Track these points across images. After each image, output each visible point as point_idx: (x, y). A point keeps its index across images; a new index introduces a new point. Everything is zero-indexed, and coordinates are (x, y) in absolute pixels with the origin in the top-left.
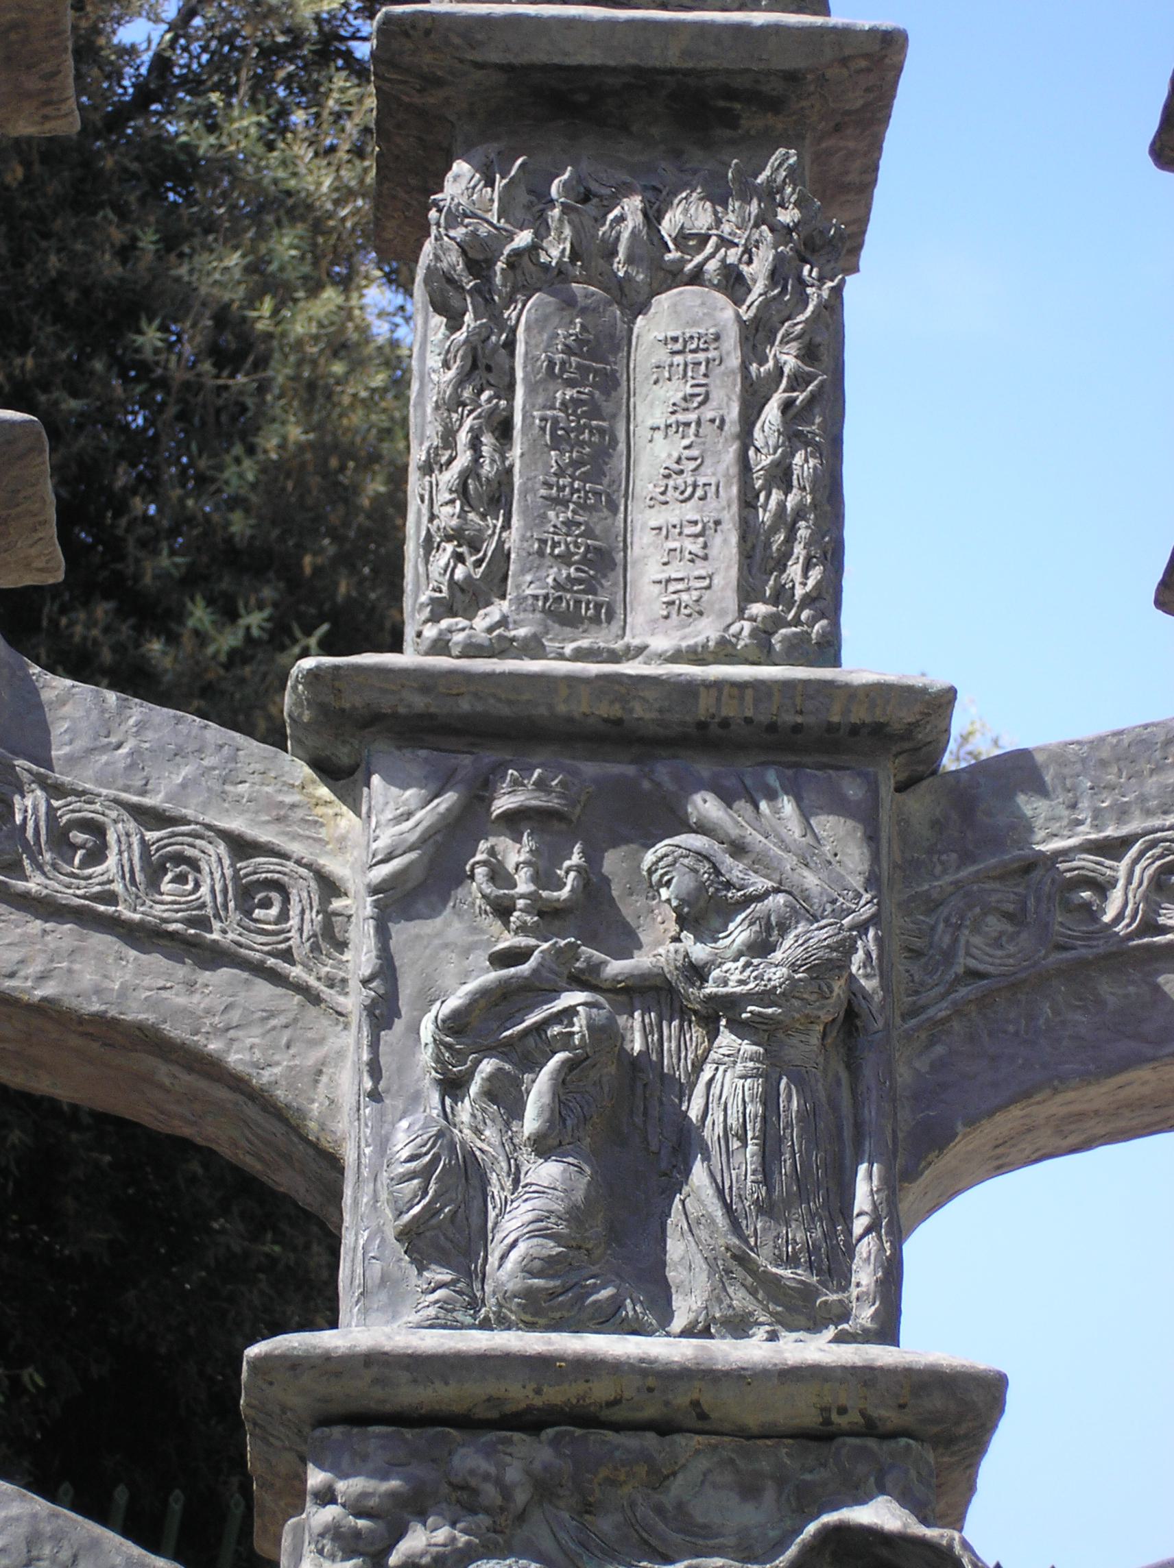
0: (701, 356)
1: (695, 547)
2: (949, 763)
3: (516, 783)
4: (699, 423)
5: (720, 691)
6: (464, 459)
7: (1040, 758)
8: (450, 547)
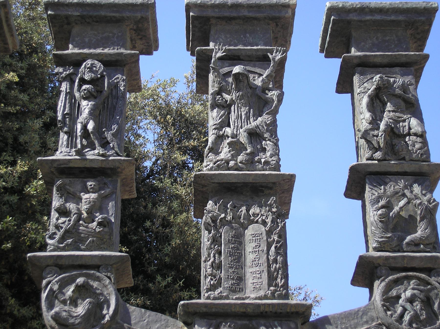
0: (258, 238)
1: (259, 276)
2: (312, 319)
3: (224, 326)
4: (258, 251)
5: (265, 306)
6: (212, 259)
7: (330, 317)
8: (210, 277)
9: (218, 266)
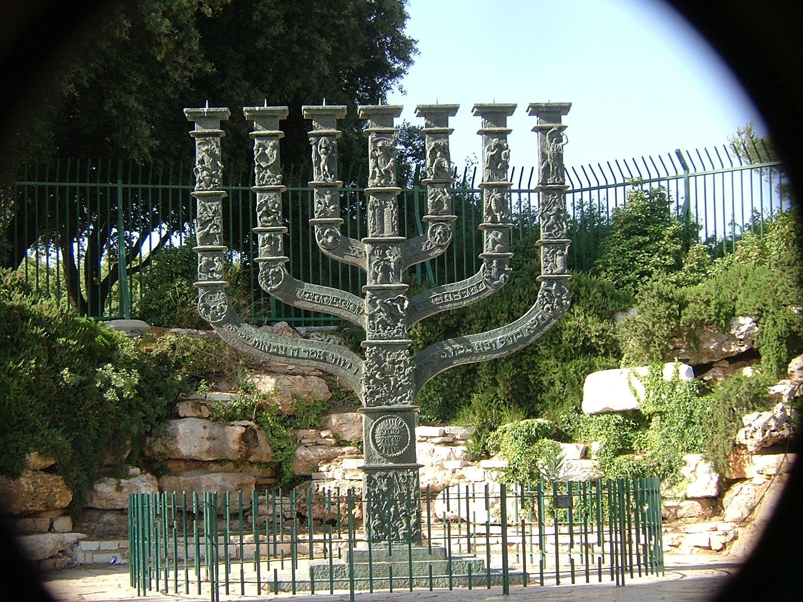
9: (374, 224)
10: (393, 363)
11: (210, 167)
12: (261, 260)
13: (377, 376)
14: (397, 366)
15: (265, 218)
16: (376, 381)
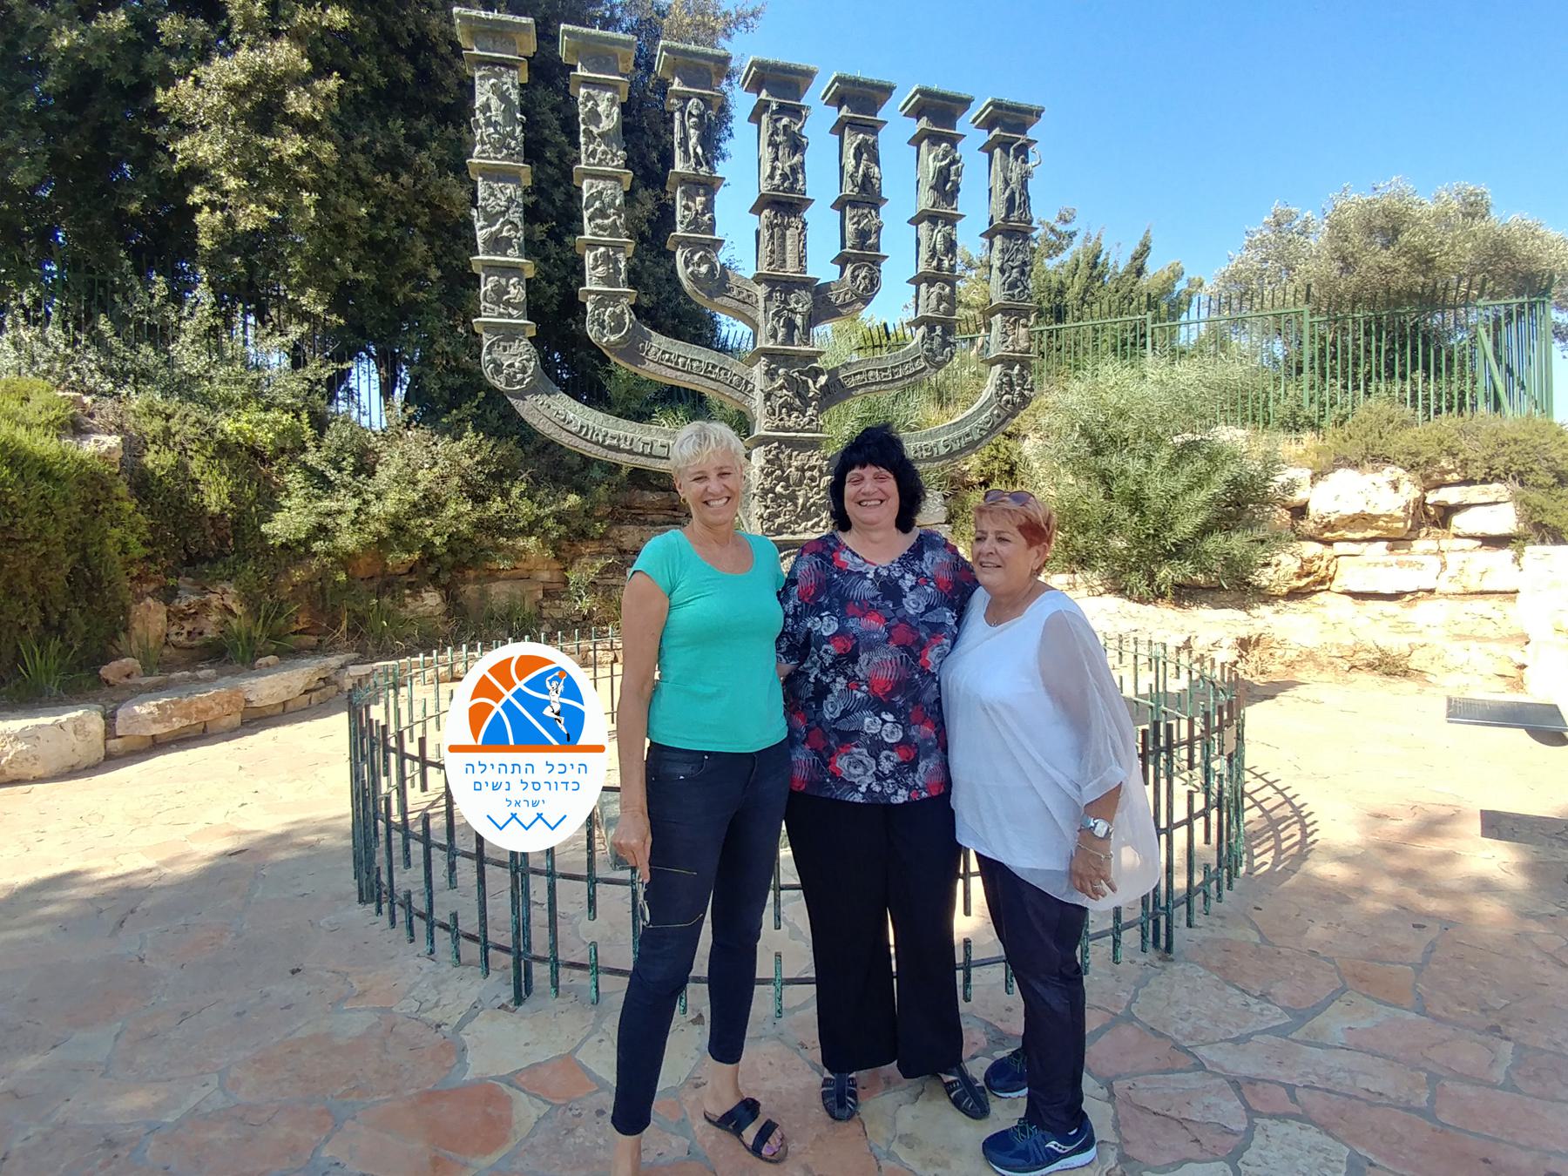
10: (802, 469)
11: (500, 119)
12: (591, 292)
13: (779, 489)
14: (808, 474)
15: (599, 221)
16: (778, 496)
